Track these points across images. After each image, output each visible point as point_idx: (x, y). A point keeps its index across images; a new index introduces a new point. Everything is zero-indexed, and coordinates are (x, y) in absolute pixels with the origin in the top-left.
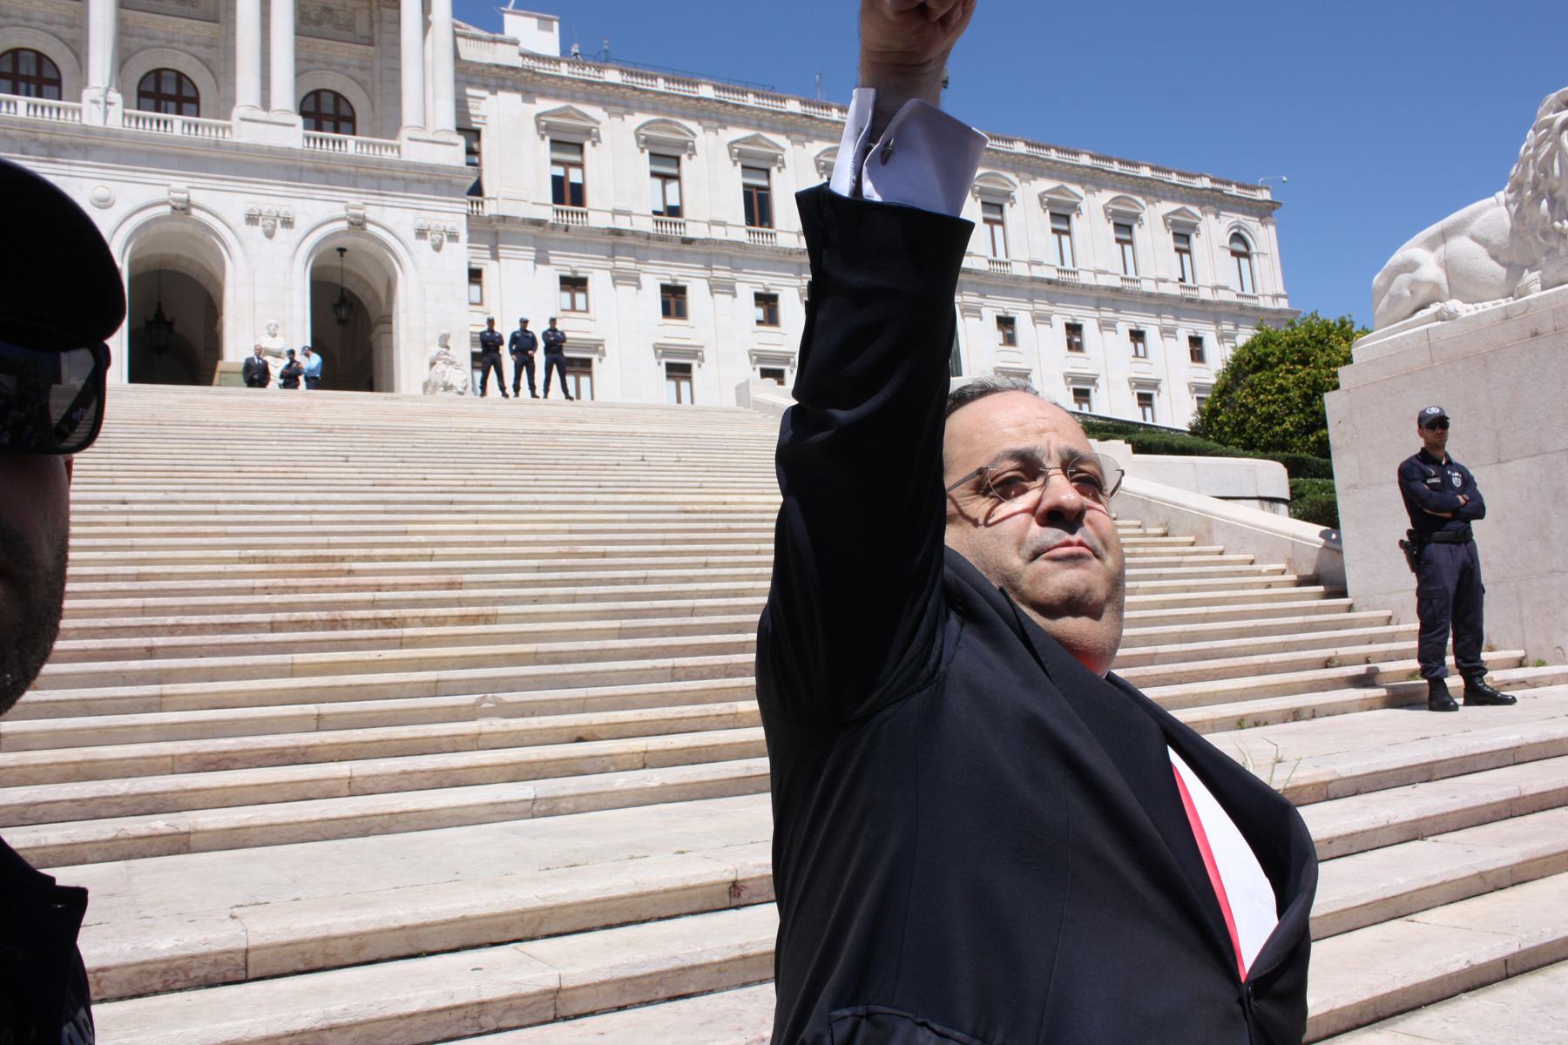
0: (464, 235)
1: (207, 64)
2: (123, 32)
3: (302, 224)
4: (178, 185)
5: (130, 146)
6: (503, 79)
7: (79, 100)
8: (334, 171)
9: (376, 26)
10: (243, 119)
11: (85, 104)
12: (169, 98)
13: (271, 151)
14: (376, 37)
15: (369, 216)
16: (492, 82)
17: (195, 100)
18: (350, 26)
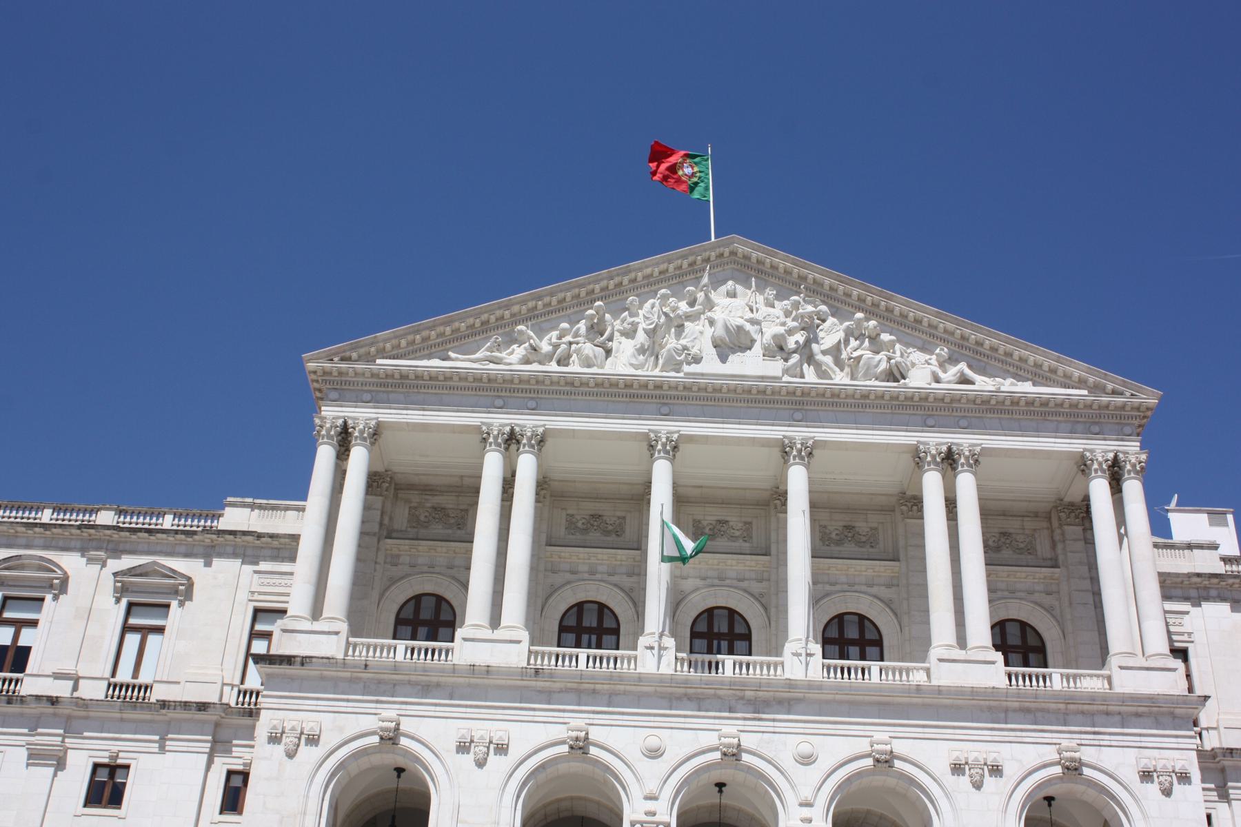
0: (1196, 775)
1: (888, 603)
2: (817, 579)
3: (1012, 771)
4: (882, 735)
5: (830, 697)
6: (1206, 588)
7: (778, 652)
8: (1042, 710)
9: (1060, 546)
10: (940, 660)
11: (787, 655)
12: (853, 642)
13: (974, 692)
14: (1061, 558)
15: (1085, 759)
16: (1193, 593)
17: (879, 643)
18: (1030, 550)
